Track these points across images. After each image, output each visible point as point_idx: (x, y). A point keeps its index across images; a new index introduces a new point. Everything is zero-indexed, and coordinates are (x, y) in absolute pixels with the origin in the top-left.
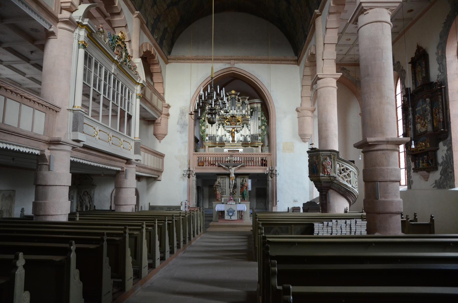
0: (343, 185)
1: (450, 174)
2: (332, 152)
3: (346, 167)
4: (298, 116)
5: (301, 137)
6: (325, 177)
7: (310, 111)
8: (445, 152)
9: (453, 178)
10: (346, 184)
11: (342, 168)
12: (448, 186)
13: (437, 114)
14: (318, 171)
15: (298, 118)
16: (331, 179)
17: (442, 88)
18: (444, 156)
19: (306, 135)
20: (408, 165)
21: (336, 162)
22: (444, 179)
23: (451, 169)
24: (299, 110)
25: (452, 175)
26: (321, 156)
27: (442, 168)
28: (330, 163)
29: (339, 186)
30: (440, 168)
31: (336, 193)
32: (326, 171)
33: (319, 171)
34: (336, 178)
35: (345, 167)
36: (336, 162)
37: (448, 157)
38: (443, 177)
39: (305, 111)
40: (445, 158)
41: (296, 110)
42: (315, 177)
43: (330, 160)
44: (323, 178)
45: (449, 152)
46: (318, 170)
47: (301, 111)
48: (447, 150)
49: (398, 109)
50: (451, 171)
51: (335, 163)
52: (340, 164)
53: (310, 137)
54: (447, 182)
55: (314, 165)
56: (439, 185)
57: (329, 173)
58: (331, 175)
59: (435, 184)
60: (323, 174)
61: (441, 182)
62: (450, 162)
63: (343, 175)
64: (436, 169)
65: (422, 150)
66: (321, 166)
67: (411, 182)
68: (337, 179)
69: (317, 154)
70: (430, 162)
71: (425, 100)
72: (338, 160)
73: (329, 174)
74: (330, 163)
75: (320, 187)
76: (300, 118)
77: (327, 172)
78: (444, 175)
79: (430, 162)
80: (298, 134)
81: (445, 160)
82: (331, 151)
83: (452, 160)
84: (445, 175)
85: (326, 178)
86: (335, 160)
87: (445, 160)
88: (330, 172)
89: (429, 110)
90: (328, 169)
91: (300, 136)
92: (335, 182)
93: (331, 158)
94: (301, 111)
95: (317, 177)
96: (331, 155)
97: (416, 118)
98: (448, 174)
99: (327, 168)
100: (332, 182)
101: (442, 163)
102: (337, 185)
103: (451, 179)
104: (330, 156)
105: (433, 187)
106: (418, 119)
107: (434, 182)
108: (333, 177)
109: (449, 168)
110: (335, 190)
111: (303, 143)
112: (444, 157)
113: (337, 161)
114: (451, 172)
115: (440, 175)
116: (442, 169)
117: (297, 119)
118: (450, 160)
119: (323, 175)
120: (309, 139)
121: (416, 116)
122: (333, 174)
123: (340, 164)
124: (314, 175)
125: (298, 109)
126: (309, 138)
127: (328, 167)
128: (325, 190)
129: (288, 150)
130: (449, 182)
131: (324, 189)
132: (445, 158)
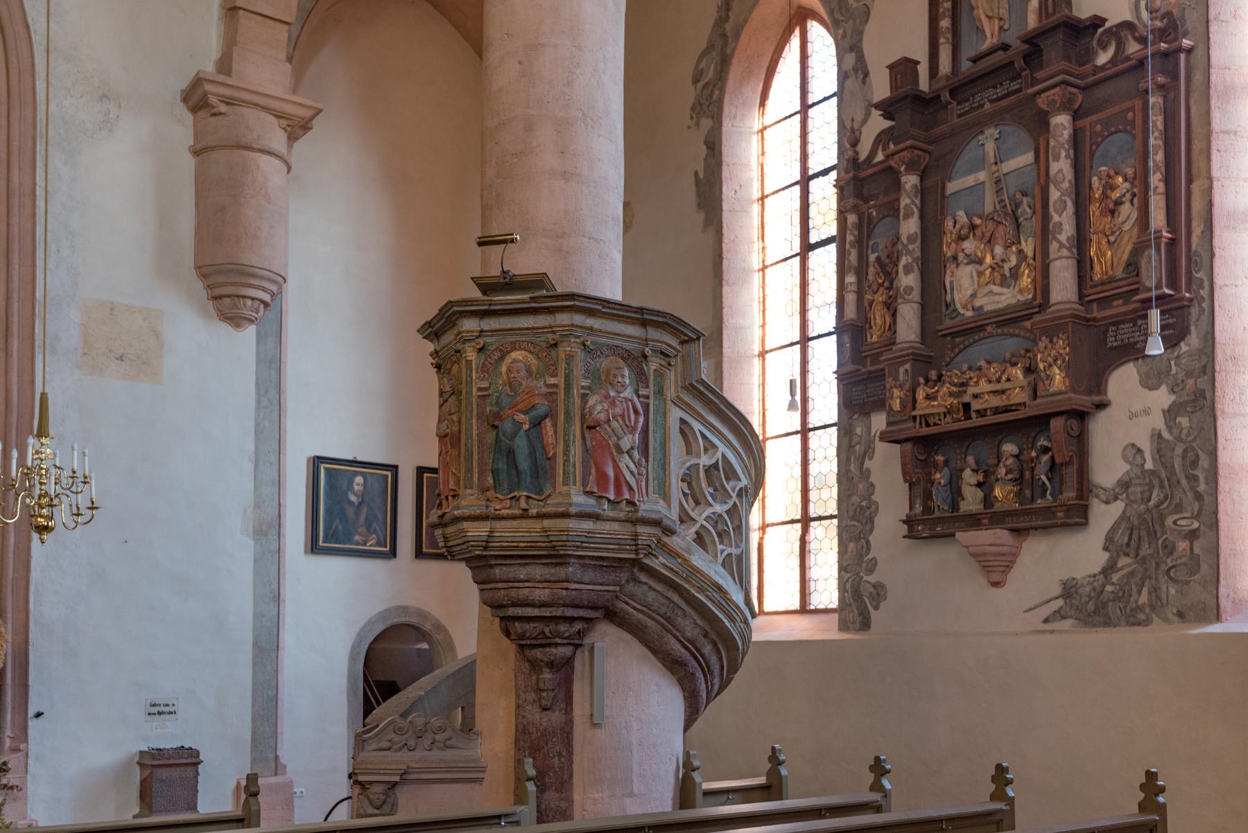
0: (702, 590)
1: (1182, 545)
2: (653, 333)
3: (723, 456)
4: (197, 136)
5: (209, 287)
6: (600, 526)
7: (284, 122)
8: (1158, 422)
9: (1204, 568)
10: (721, 582)
11: (705, 460)
12: (1170, 612)
13: (1118, 203)
14: (553, 468)
15: (196, 153)
16: (636, 536)
17: (1180, 49)
18: (1146, 445)
19: (243, 274)
20: (855, 499)
21: (676, 414)
22: (1132, 574)
23: (1197, 516)
24: (213, 100)
25: (1197, 551)
26: (579, 353)
27: (1120, 512)
28: (636, 412)
29: (675, 598)
30: (1104, 516)
31: (638, 648)
32: (611, 473)
33: (560, 478)
34: (669, 531)
35: (719, 455)
36: (676, 414)
37: (1179, 450)
38: (1123, 561)
39: (252, 115)
40: (1148, 456)
41: (185, 100)
42: (525, 515)
43: (639, 396)
44: (588, 525)
45: (1183, 421)
46: (552, 459)
47: (223, 108)
48: (1171, 413)
49: (814, 185)
50: (1196, 525)
51: (665, 414)
52: (697, 426)
53: (273, 295)
54: (1155, 590)
55: (521, 417)
56: (1091, 607)
57: (630, 488)
58: (642, 507)
59: (1060, 602)
60: (589, 493)
61: (1109, 588)
62: (1193, 479)
63: (709, 511)
64: (1077, 517)
65: (1007, 409)
66: (576, 428)
67: (866, 590)
68: (675, 542)
69: (551, 329)
70: (1043, 477)
71: (1047, 124)
72: (687, 399)
73: (631, 503)
74: (636, 412)
75: (543, 605)
76: (216, 155)
77: (619, 481)
78: (1138, 548)
79: (1043, 477)
80: (189, 261)
81: (1149, 465)
82: (644, 323)
83: (1204, 462)
84: (1145, 550)
85: (607, 526)
86: (671, 393)
87: (1149, 465)
88: (633, 482)
89: (1070, 182)
90: (626, 455)
91: (204, 276)
92: (658, 562)
93: (641, 377)
94: (223, 108)
95: (541, 516)
96: (647, 350)
97: (948, 238)
98: (1170, 549)
99: (619, 449)
100: (635, 563)
101: (1125, 484)
102: (659, 587)
103: (1192, 574)
104: (637, 361)
105: (1046, 621)
106: (961, 238)
107: (1057, 590)
108: (656, 523)
109: (1179, 508)
110: (637, 631)
111: (226, 328)
112: (1139, 451)
113: (679, 403)
114: (1192, 535)
115: (1106, 549)
116: (1124, 517)
117: (189, 162)
118: (1195, 463)
119: (592, 501)
120: (266, 305)
121: (949, 224)
122: (650, 506)
123: (697, 426)
124: (518, 499)
125: (208, 87)
126: (267, 297)
127: (626, 443)
128: (579, 626)
129: (121, 358)
130: (1172, 591)
131: (572, 620)
132: (1148, 456)
